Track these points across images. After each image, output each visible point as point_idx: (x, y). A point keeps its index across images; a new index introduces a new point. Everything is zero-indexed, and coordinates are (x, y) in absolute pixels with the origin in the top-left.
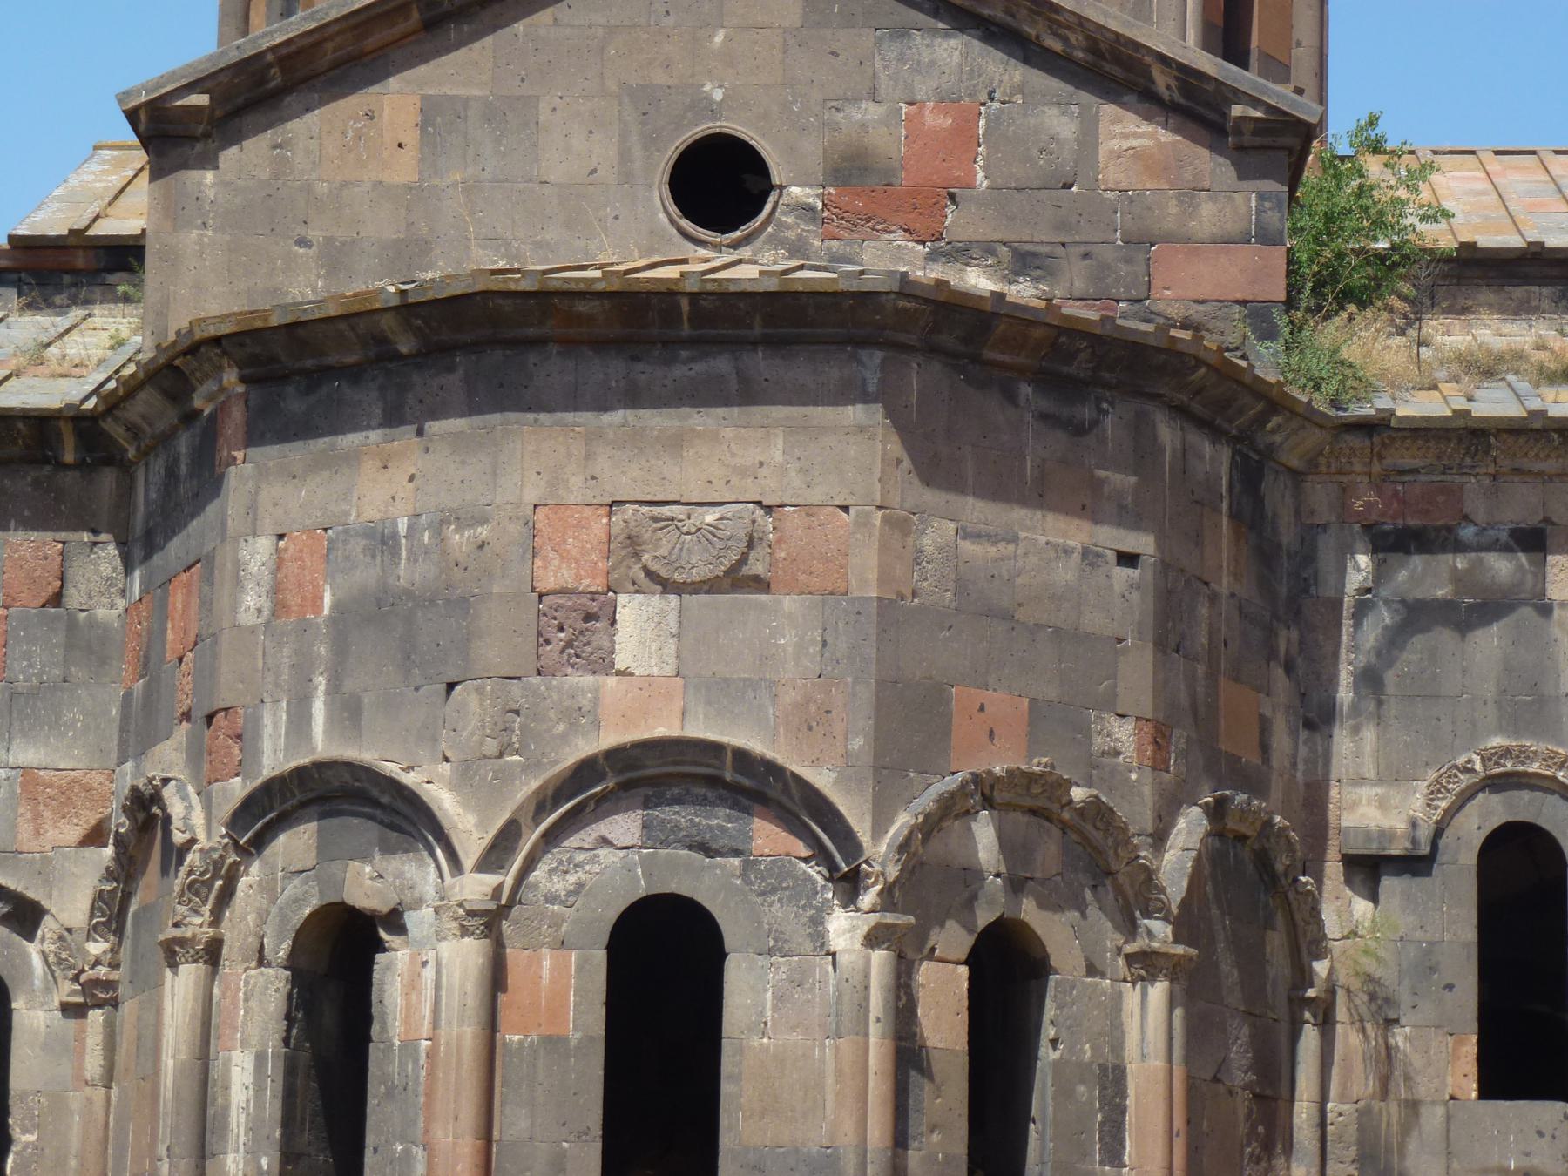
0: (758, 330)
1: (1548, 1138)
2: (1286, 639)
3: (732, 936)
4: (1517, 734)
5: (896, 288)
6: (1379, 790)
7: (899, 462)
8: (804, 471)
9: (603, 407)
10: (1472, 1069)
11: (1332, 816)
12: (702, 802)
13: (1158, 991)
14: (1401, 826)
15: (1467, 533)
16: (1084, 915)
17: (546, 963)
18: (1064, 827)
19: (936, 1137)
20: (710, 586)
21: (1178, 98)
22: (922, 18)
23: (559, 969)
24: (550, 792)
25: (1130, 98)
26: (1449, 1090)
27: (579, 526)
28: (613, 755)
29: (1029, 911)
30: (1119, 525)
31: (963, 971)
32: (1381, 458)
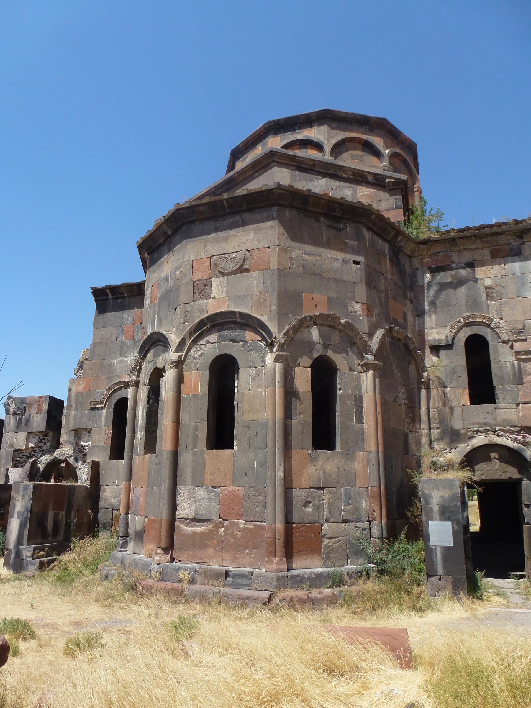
0: (245, 207)
1: (490, 414)
2: (410, 294)
3: (241, 362)
4: (471, 312)
5: (277, 187)
6: (437, 330)
7: (283, 234)
8: (258, 240)
9: (209, 234)
10: (468, 397)
11: (426, 338)
12: (233, 329)
13: (370, 374)
14: (443, 337)
15: (454, 265)
16: (348, 355)
17: (193, 375)
18: (340, 331)
19: (301, 416)
20: (234, 272)
21: (374, 182)
22: (316, 177)
23: (197, 376)
24: (193, 330)
25: (363, 184)
26: (462, 403)
27: (203, 263)
28: (207, 318)
29: (330, 353)
30: (353, 254)
31: (309, 370)
32: (430, 250)
